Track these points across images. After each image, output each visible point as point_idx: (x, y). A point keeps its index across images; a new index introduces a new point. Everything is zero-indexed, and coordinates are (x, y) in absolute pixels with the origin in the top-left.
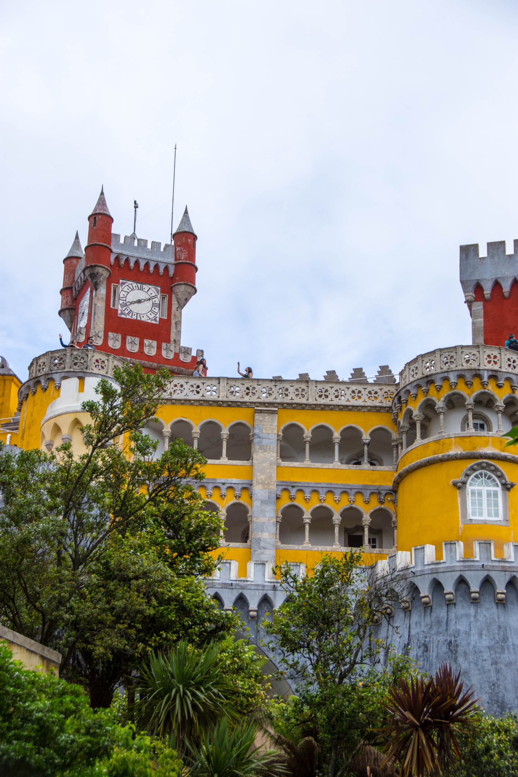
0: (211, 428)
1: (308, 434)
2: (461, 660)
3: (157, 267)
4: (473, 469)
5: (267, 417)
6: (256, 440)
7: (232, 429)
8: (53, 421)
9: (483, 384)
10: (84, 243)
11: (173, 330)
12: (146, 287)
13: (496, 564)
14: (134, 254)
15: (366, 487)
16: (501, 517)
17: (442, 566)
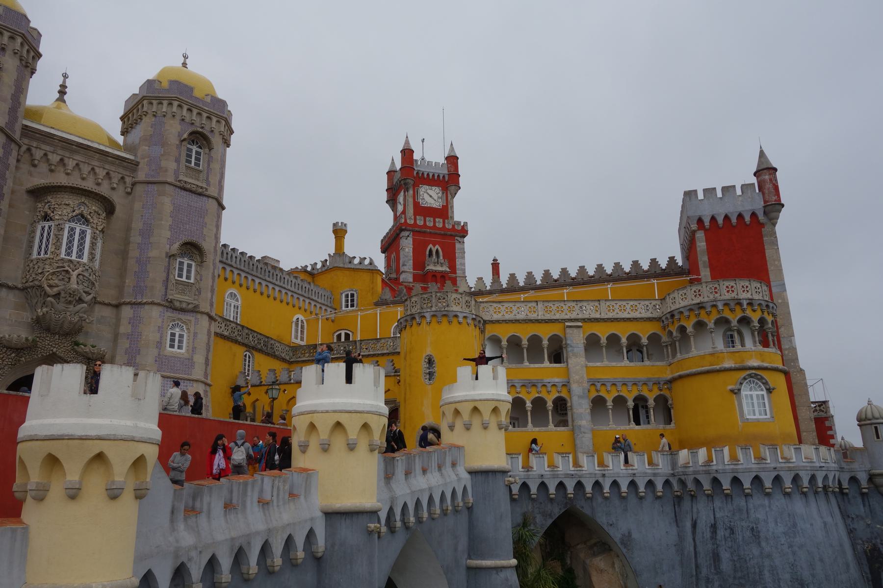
0: (535, 340)
1: (604, 341)
2: (763, 544)
3: (438, 176)
4: (745, 379)
5: (575, 330)
6: (569, 349)
7: (550, 339)
8: (454, 406)
9: (743, 310)
10: (398, 166)
11: (450, 211)
12: (434, 188)
13: (783, 465)
14: (425, 170)
15: (649, 380)
16: (768, 416)
17: (740, 467)
